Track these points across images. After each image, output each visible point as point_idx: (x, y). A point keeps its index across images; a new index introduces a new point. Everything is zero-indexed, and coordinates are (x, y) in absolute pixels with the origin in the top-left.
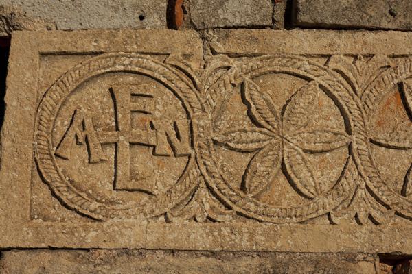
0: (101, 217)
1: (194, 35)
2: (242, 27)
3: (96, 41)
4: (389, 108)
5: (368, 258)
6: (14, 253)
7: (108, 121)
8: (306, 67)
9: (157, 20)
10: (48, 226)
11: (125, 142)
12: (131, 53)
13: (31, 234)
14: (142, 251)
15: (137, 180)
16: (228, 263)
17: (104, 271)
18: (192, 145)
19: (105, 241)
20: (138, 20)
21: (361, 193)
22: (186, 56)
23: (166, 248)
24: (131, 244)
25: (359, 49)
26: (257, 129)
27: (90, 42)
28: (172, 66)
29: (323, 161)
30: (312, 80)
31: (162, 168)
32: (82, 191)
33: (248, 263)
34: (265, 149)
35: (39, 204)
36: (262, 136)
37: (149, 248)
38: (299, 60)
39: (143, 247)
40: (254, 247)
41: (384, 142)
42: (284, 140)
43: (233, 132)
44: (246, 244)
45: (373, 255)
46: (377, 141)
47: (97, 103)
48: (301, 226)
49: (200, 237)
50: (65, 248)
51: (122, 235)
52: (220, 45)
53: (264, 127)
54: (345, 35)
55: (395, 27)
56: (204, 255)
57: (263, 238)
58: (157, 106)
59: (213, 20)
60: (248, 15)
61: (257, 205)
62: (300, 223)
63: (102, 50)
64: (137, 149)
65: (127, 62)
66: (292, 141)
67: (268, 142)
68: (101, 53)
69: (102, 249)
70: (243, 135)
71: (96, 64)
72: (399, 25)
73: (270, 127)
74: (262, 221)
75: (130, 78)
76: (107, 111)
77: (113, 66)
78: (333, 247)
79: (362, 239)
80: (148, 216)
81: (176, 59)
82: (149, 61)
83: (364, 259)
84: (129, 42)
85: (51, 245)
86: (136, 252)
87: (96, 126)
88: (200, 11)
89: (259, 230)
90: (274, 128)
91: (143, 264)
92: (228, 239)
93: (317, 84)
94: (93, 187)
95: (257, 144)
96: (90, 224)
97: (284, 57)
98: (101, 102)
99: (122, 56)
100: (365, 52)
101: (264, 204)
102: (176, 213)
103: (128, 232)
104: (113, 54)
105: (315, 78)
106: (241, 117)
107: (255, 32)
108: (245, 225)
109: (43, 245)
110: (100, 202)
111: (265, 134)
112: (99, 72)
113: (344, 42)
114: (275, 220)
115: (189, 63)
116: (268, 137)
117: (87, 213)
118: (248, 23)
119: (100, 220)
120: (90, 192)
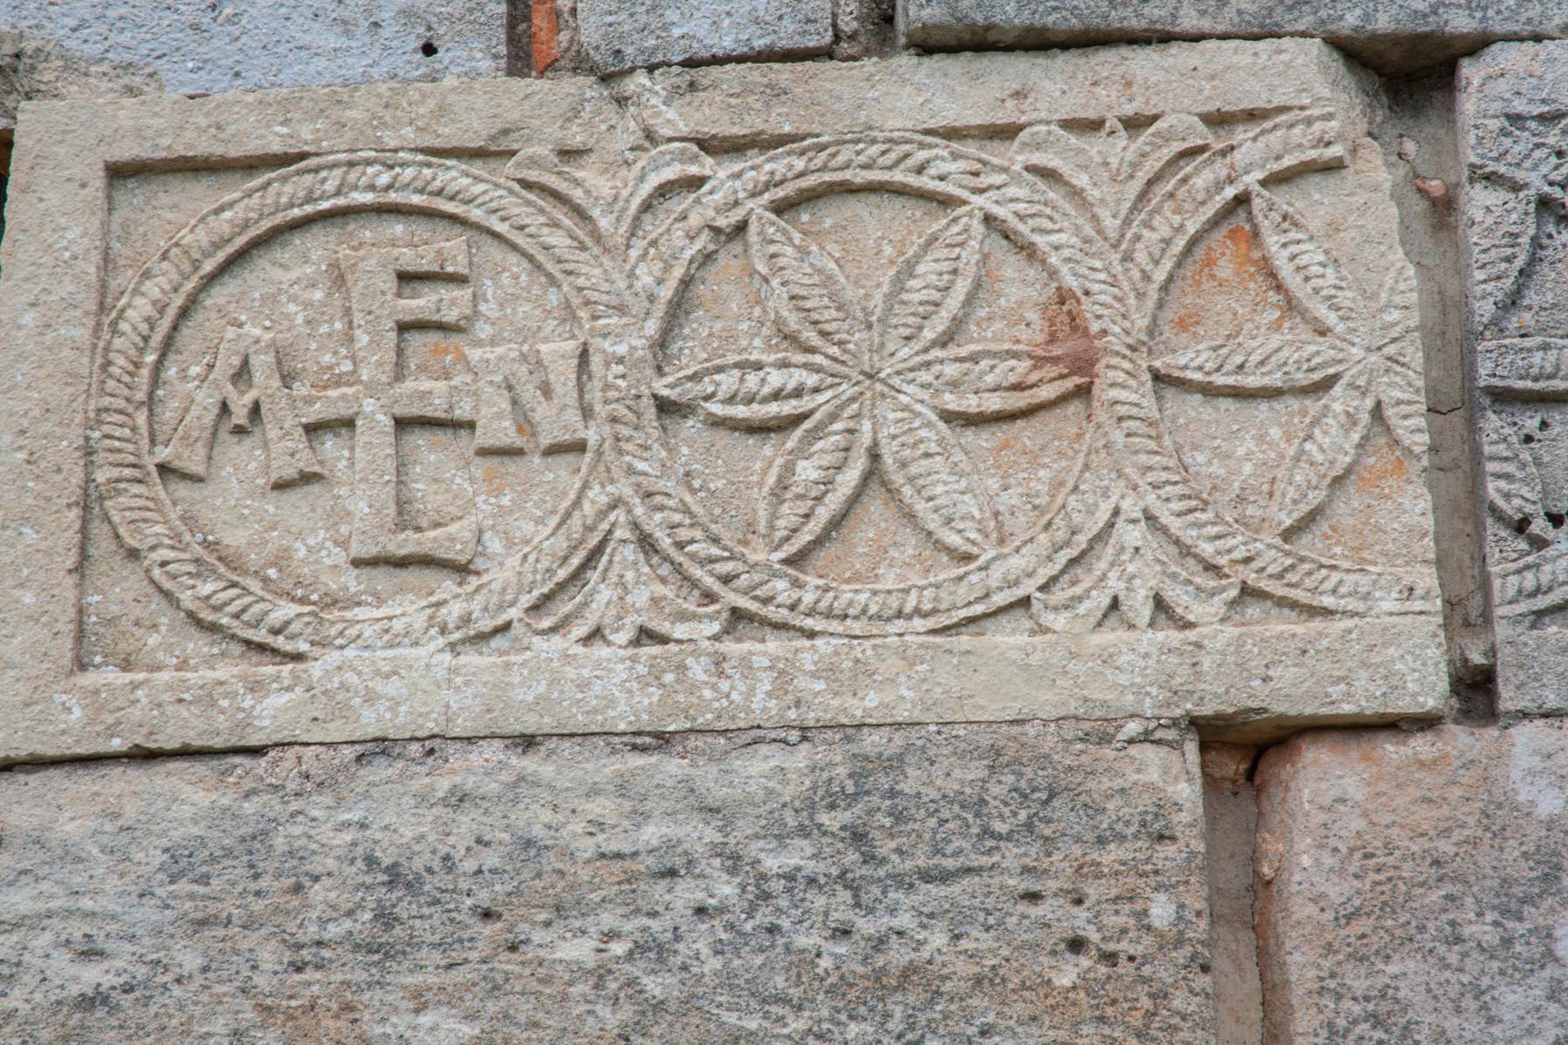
0: (303, 647)
1: (585, 85)
2: (741, 59)
3: (284, 123)
4: (1213, 277)
5: (1158, 735)
6: (22, 778)
7: (327, 358)
8: (946, 168)
9: (475, 54)
10: (135, 686)
11: (380, 417)
12: (395, 151)
13: (77, 713)
14: (433, 745)
15: (418, 529)
16: (713, 770)
17: (315, 813)
18: (587, 413)
19: (315, 719)
20: (420, 55)
21: (1132, 535)
22: (568, 154)
23: (507, 731)
24: (397, 723)
25: (1110, 102)
26: (799, 358)
27: (268, 126)
28: (526, 185)
29: (1005, 446)
30: (965, 203)
31: (499, 492)
32: (246, 573)
33: (773, 763)
34: (818, 416)
35: (110, 622)
36: (811, 380)
37: (457, 732)
38: (922, 146)
39: (436, 731)
40: (792, 714)
41: (1198, 376)
42: (879, 387)
43: (720, 369)
44: (762, 704)
45: (1175, 723)
46: (1177, 373)
47: (292, 308)
48: (938, 639)
49: (616, 686)
50: (186, 753)
51: (370, 698)
52: (671, 114)
53: (812, 350)
54: (1062, 62)
55: (1221, 28)
56: (635, 747)
57: (820, 686)
58: (483, 308)
59: (652, 42)
60: (756, 21)
61: (797, 584)
62: (934, 632)
63: (306, 148)
64: (419, 440)
65: (384, 179)
66: (905, 387)
67: (829, 394)
68: (303, 156)
69: (307, 744)
70: (752, 379)
71: (285, 194)
72: (1236, 19)
73: (834, 350)
74: (811, 635)
75: (398, 228)
76: (324, 329)
77: (338, 193)
78: (1046, 701)
79: (1135, 670)
80: (457, 636)
81: (534, 162)
82: (453, 175)
83: (1146, 738)
84: (387, 118)
85: (139, 740)
86: (415, 749)
87: (287, 379)
88: (609, 19)
89: (807, 661)
90: (845, 351)
91: (443, 785)
92: (708, 694)
93: (979, 214)
94: (281, 559)
95: (794, 402)
96: (270, 670)
97: (874, 141)
98: (307, 305)
99: (369, 162)
100: (1129, 109)
101: (821, 582)
102: (546, 623)
103: (392, 688)
104: (342, 157)
105: (974, 199)
106: (744, 326)
107: (783, 73)
108: (758, 647)
109: (116, 744)
110: (303, 601)
111: (818, 369)
112: (296, 212)
113: (1058, 85)
114: (856, 627)
115: (580, 174)
116: (829, 380)
117: (260, 636)
118: (759, 44)
119: (298, 657)
120: (272, 573)
